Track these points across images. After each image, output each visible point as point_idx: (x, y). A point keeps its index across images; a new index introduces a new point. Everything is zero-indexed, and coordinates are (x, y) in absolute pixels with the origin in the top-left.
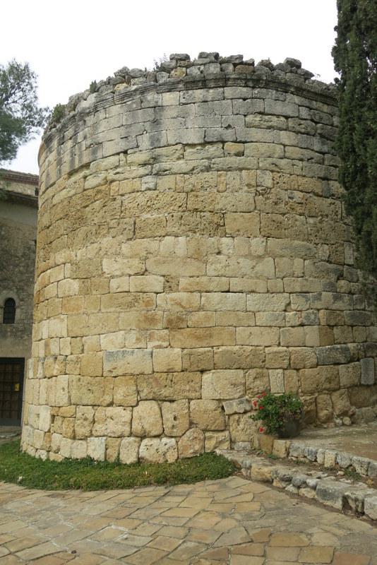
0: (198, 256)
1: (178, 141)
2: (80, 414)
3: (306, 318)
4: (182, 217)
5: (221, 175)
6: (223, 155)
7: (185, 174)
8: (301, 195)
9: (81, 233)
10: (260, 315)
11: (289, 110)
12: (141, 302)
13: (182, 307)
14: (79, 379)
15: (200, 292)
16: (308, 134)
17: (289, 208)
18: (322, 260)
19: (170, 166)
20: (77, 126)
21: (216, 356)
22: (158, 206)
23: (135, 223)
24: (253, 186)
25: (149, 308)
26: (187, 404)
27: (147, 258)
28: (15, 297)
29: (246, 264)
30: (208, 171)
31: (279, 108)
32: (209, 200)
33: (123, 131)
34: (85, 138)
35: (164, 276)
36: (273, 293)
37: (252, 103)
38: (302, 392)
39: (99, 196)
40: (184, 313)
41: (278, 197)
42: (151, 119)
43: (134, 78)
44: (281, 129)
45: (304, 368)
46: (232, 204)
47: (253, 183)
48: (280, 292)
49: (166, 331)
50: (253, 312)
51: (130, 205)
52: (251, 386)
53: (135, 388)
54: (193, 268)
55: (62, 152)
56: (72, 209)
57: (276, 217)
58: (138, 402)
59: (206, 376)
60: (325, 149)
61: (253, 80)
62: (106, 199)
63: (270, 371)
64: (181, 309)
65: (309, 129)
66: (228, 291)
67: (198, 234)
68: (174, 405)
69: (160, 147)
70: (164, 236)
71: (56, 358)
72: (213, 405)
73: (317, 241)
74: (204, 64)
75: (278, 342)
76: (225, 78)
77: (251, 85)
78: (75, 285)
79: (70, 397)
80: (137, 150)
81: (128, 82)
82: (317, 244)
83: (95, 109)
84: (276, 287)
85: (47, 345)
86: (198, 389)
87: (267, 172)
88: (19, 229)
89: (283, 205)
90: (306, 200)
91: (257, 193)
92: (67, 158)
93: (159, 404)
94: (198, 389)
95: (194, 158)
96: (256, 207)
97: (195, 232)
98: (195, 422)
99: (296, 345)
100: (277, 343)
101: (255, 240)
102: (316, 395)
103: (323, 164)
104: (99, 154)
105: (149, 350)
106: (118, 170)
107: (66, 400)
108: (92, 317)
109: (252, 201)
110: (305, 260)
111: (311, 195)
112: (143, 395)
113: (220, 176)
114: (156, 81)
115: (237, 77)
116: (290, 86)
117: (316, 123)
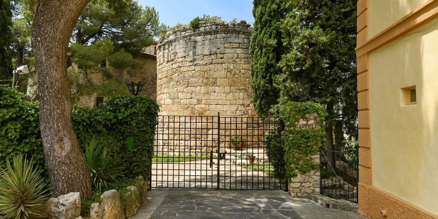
3: (243, 113)
11: (240, 41)
20: (169, 45)
31: (236, 41)
34: (172, 50)
37: (227, 39)
42: (193, 46)
43: (187, 30)
44: (237, 48)
47: (226, 68)
51: (187, 75)
54: (206, 97)
56: (169, 75)
61: (227, 32)
74: (211, 26)
78: (170, 101)
81: (186, 31)
91: (228, 72)
92: (166, 56)
95: (207, 60)
104: (177, 57)
106: (183, 63)
109: (226, 74)
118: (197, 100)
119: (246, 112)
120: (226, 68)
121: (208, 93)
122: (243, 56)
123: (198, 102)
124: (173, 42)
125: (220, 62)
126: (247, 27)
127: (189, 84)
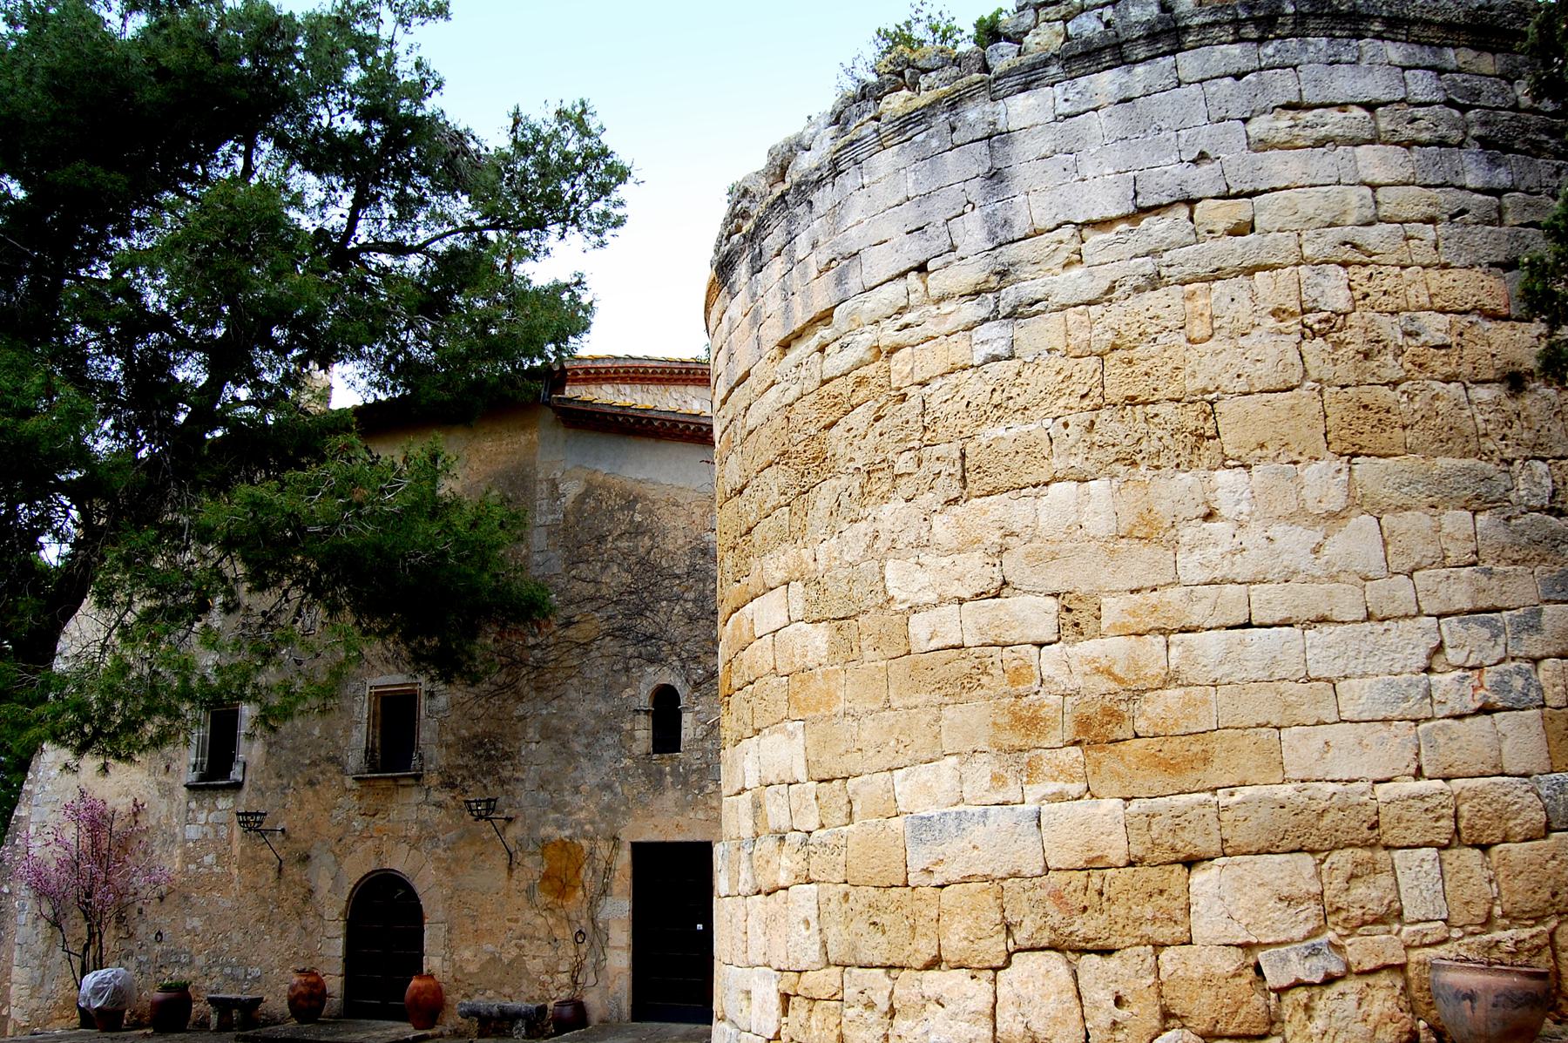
1: (1061, 218)
2: (854, 990)
4: (1093, 423)
5: (1194, 293)
6: (1192, 238)
7: (1089, 303)
9: (824, 497)
10: (1350, 688)
11: (1375, 86)
13: (1116, 679)
14: (846, 895)
15: (1163, 632)
16: (1442, 143)
17: (1408, 366)
18: (1531, 509)
19: (1044, 290)
21: (1225, 816)
22: (1021, 401)
23: (963, 456)
24: (1293, 314)
25: (1021, 688)
26: (1151, 960)
28: (678, 683)
29: (1294, 541)
30: (1155, 289)
31: (1345, 84)
32: (1167, 369)
33: (910, 216)
34: (814, 246)
35: (1056, 595)
36: (1383, 620)
38: (1504, 915)
39: (862, 393)
41: (1372, 335)
43: (925, 71)
45: (1504, 841)
46: (1233, 372)
47: (1293, 305)
48: (1406, 616)
49: (1075, 752)
50: (1329, 680)
51: (947, 408)
52: (1342, 902)
53: (999, 917)
54: (1141, 563)
55: (760, 292)
56: (797, 437)
58: (1009, 955)
59: (1199, 877)
60: (1502, 178)
61: (1257, 22)
62: (882, 400)
63: (1397, 854)
64: (1113, 686)
65: (1443, 130)
66: (1248, 625)
67: (1143, 469)
68: (1113, 962)
69: (1013, 242)
70: (1046, 484)
71: (782, 839)
72: (1227, 962)
73: (1508, 454)
75: (1414, 765)
76: (1177, 29)
77: (1254, 35)
78: (819, 638)
79: (824, 944)
80: (952, 257)
81: (914, 86)
82: (1510, 462)
83: (835, 169)
85: (757, 806)
86: (1179, 915)
87: (1331, 269)
88: (676, 504)
89: (1390, 357)
90: (1461, 334)
92: (773, 305)
93: (1069, 962)
94: (1179, 915)
96: (1305, 371)
97: (1134, 463)
98: (1178, 1012)
99: (1472, 771)
100: (1412, 770)
101: (1314, 466)
102: (1553, 923)
103: (1500, 221)
104: (854, 284)
105: (1030, 807)
106: (908, 318)
107: (814, 953)
108: (868, 721)
109: (1292, 356)
110: (1475, 512)
111: (1474, 318)
112: (1021, 936)
113: (1190, 297)
114: (986, 69)
115: (1210, 19)
116: (1369, 18)
117: (1464, 109)
119: (1518, 683)
120: (1293, 305)
122: (1411, 201)
123: (1069, 617)
124: (819, 183)
127: (970, 477)
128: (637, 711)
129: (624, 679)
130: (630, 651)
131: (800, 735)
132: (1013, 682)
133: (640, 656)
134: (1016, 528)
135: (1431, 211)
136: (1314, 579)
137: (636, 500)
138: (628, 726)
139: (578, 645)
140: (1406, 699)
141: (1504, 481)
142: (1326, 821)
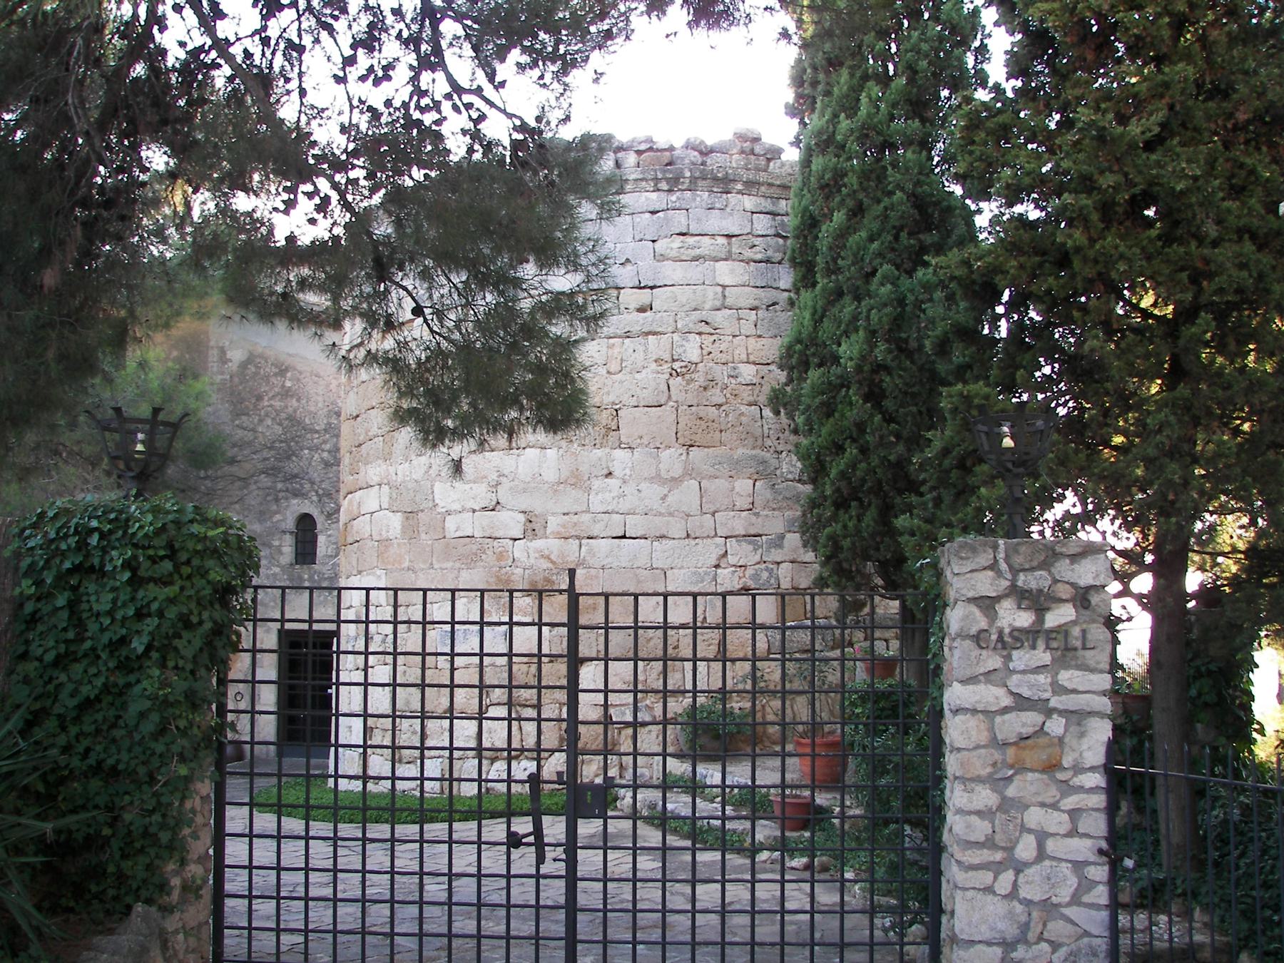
0: (577, 480)
8: (753, 368)
12: (490, 552)
13: (553, 562)
15: (578, 537)
16: (768, 261)
25: (503, 563)
27: (498, 484)
28: (315, 513)
29: (652, 493)
31: (716, 222)
40: (555, 571)
41: (710, 377)
44: (717, 260)
54: (570, 499)
57: (702, 411)
61: (668, 180)
64: (550, 565)
65: (770, 253)
66: (624, 537)
73: (779, 448)
77: (666, 188)
84: (702, 527)
88: (318, 376)
91: (674, 373)
113: (610, 347)
115: (641, 176)
118: (522, 518)
120: (667, 357)
121: (577, 480)
123: (530, 526)
125: (636, 329)
126: (769, 160)
128: (284, 532)
129: (275, 507)
130: (280, 486)
131: (383, 577)
132: (499, 559)
133: (287, 490)
134: (506, 472)
135: (756, 303)
136: (661, 514)
137: (287, 370)
138: (276, 543)
139: (240, 479)
140: (702, 581)
141: (774, 462)
142: (652, 643)
